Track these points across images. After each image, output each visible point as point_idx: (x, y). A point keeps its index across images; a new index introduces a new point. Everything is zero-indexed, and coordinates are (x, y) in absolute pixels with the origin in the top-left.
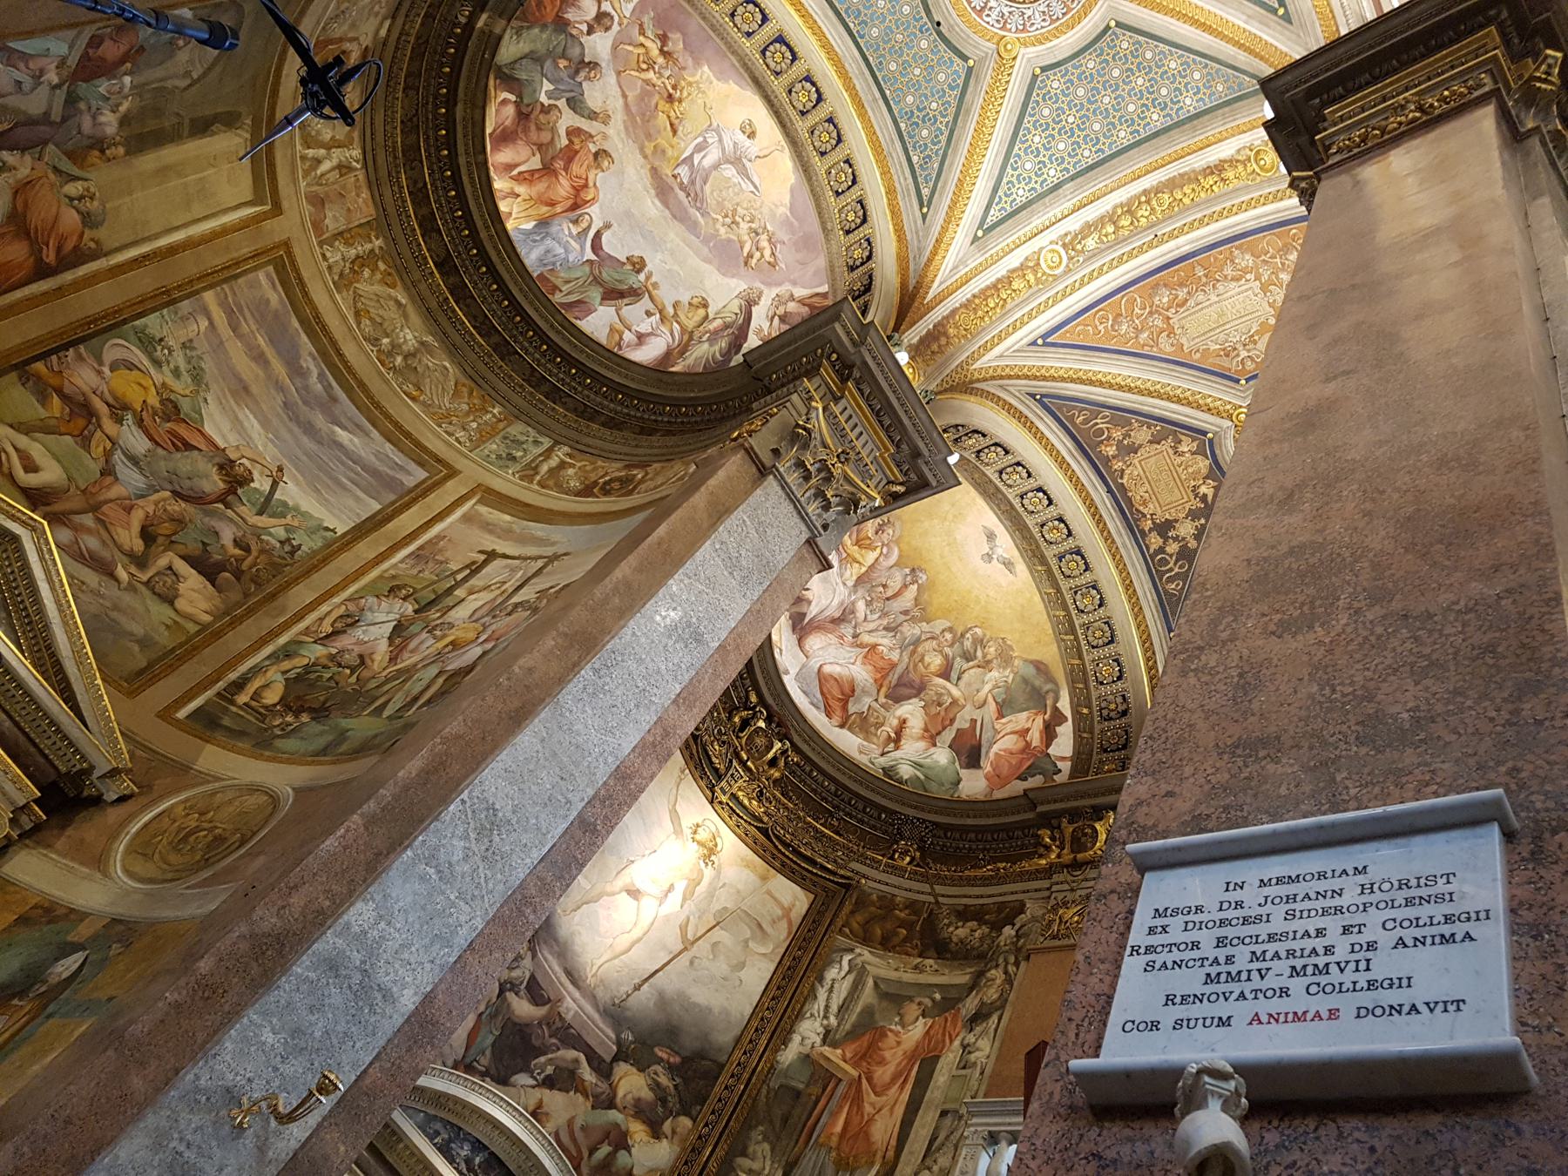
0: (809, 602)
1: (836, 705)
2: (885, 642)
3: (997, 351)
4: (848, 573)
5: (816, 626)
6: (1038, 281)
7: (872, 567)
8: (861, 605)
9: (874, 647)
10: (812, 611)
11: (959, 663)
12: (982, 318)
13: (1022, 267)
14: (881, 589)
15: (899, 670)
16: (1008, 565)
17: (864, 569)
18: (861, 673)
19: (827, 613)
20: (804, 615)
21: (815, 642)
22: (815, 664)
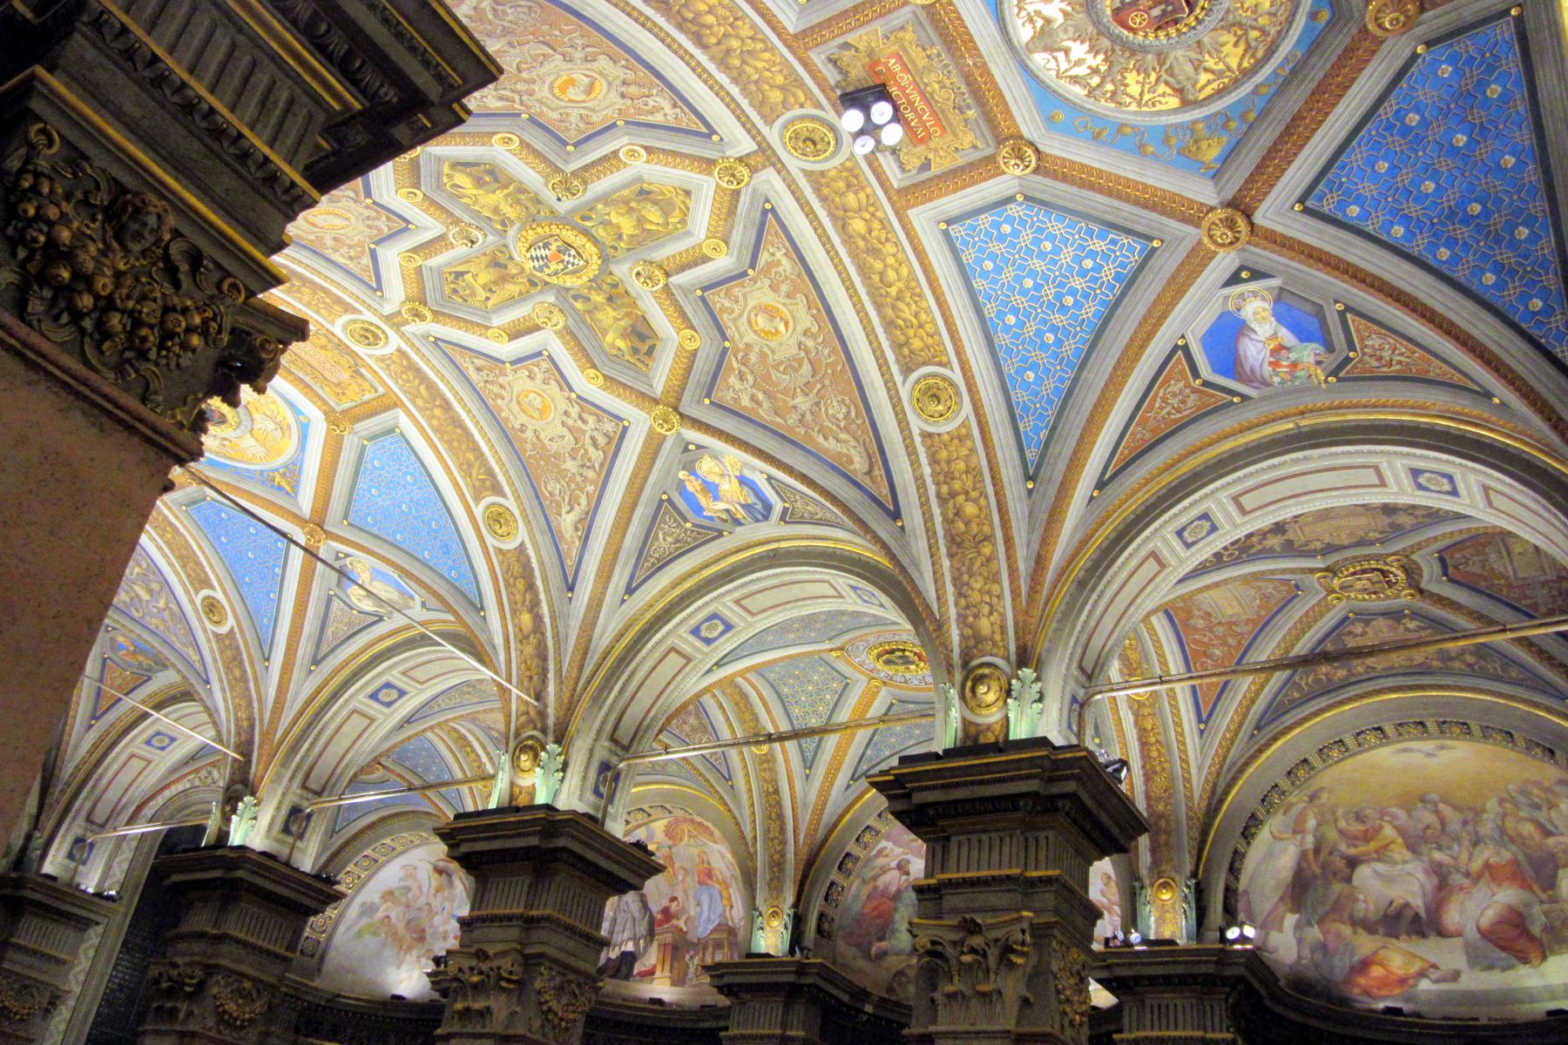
0: (1407, 905)
1: (1522, 944)
2: (1486, 854)
3: (1194, 771)
4: (1396, 856)
5: (1436, 907)
6: (1151, 706)
7: (1401, 832)
8: (1438, 856)
9: (1487, 865)
10: (1418, 903)
11: (1541, 816)
12: (1163, 769)
13: (1136, 715)
14: (1429, 832)
15: (1521, 858)
16: (1442, 748)
17: (1400, 840)
18: (1508, 895)
19: (1429, 888)
20: (1417, 915)
21: (1452, 916)
22: (1471, 932)
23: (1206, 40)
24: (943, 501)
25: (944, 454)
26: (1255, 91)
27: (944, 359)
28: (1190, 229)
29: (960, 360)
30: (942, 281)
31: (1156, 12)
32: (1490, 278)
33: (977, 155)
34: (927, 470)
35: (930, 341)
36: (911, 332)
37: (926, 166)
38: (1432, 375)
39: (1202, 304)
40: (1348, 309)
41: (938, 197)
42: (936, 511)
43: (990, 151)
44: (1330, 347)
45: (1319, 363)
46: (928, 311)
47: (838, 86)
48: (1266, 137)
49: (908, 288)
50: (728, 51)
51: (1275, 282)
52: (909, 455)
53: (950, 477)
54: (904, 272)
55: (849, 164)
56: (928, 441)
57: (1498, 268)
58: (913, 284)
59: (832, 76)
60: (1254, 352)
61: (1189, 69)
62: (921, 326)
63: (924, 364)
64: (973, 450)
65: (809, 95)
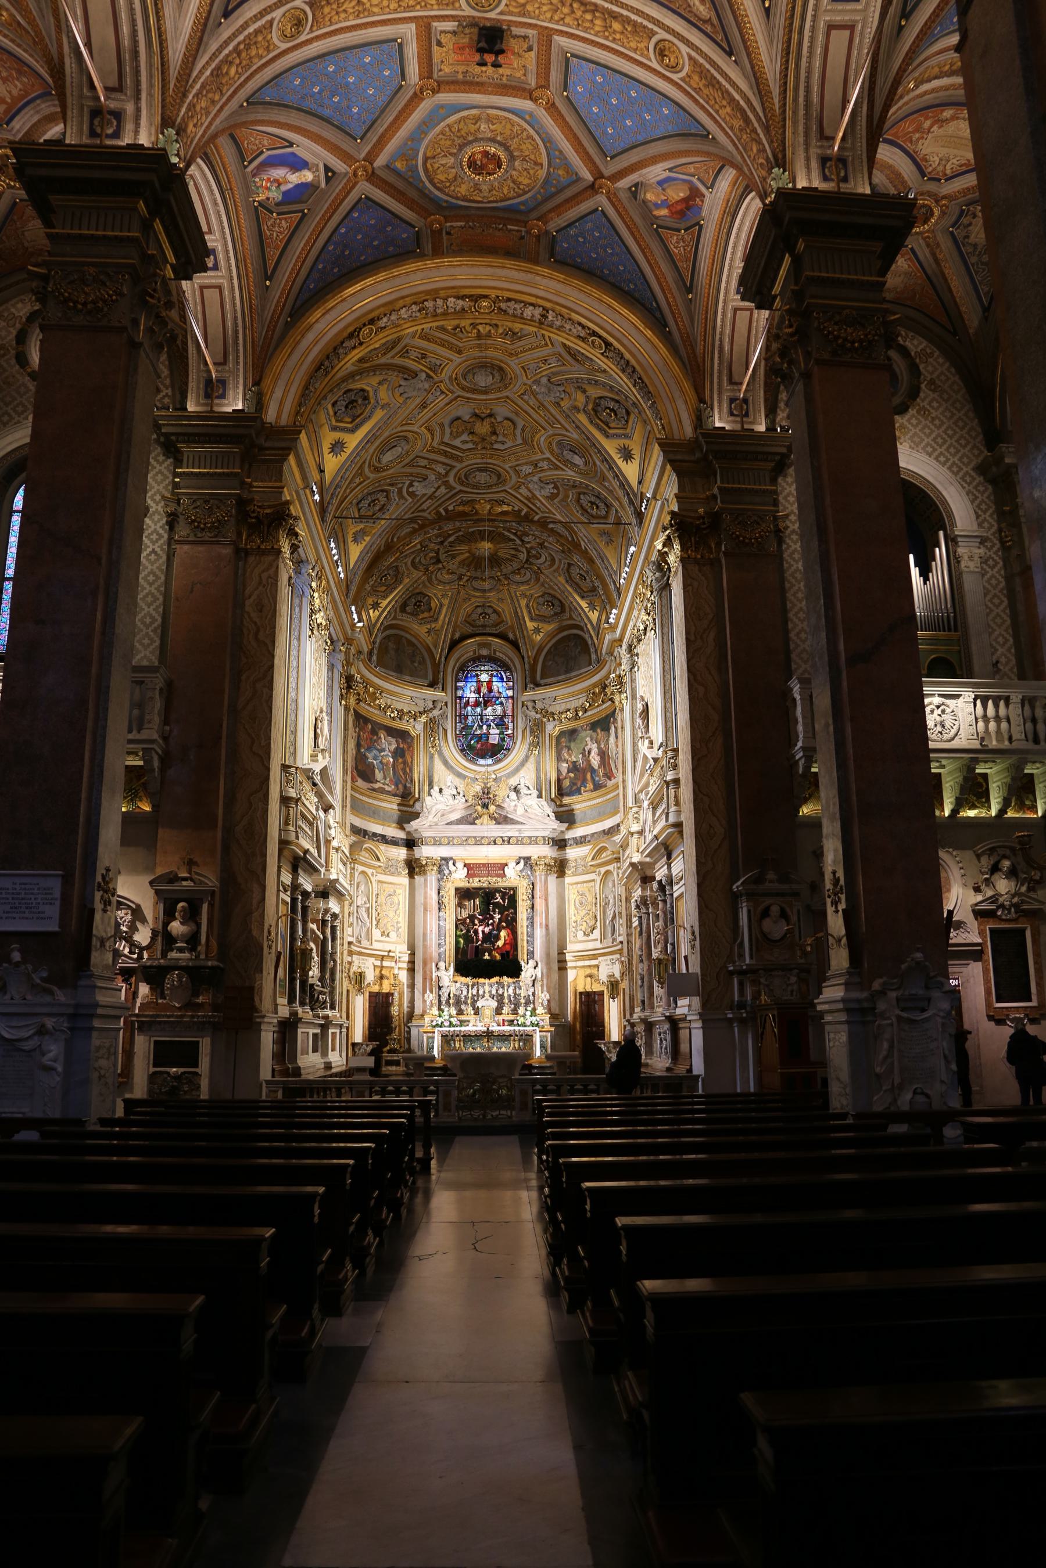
23: (454, 170)
24: (235, 49)
25: (260, 38)
26: (423, 182)
27: (315, 28)
28: (362, 156)
29: (312, 39)
30: (363, 31)
31: (479, 163)
32: (320, 266)
33: (435, 69)
34: (251, 29)
35: (327, 19)
36: (335, 6)
37: (439, 44)
38: (267, 250)
39: (314, 154)
40: (304, 215)
41: (418, 43)
42: (231, 47)
43: (435, 76)
44: (278, 204)
45: (268, 199)
46: (346, 19)
47: (509, 29)
48: (400, 185)
49: (365, 10)
50: (563, 5)
51: (323, 185)
52: (260, 13)
53: (248, 47)
54: (376, 10)
55: (457, 5)
56: (268, 26)
57: (324, 268)
58: (366, 14)
59: (516, 31)
60: (279, 173)
61: (443, 162)
62: (337, 13)
63: (314, 15)
64: (261, 57)
65: (511, 14)
